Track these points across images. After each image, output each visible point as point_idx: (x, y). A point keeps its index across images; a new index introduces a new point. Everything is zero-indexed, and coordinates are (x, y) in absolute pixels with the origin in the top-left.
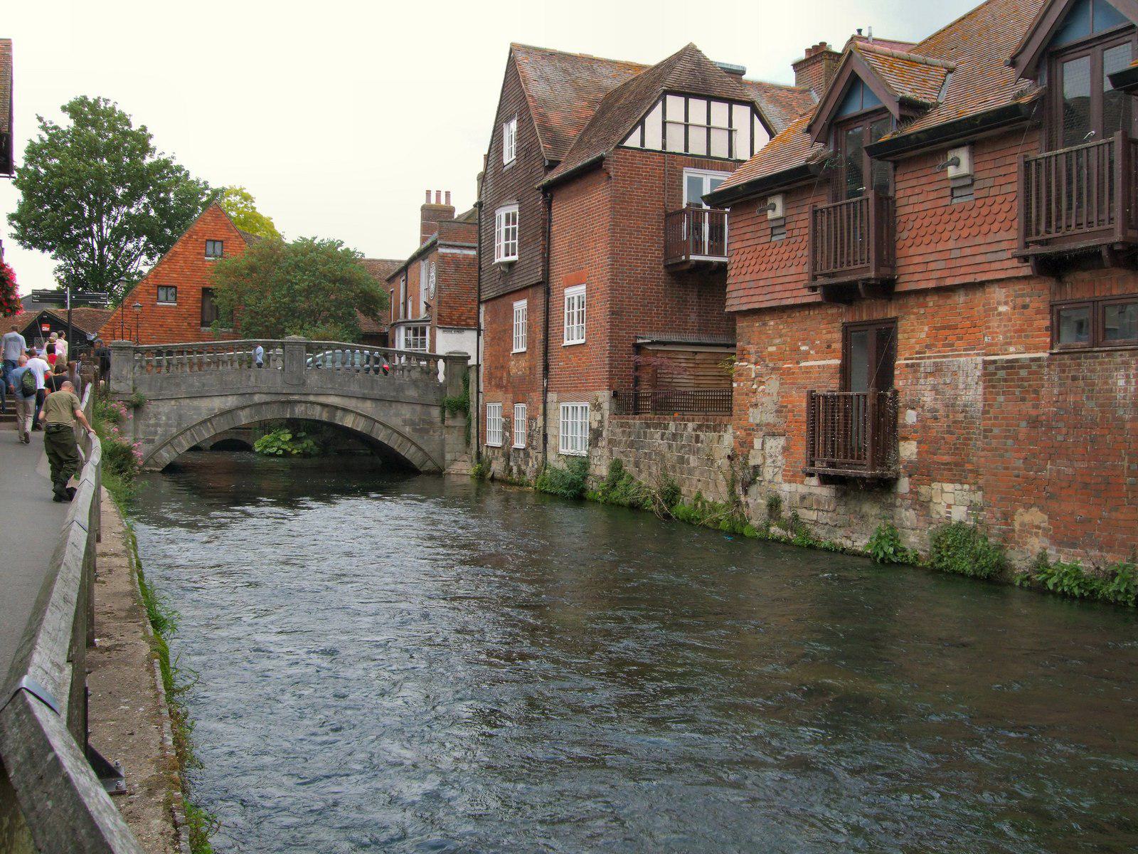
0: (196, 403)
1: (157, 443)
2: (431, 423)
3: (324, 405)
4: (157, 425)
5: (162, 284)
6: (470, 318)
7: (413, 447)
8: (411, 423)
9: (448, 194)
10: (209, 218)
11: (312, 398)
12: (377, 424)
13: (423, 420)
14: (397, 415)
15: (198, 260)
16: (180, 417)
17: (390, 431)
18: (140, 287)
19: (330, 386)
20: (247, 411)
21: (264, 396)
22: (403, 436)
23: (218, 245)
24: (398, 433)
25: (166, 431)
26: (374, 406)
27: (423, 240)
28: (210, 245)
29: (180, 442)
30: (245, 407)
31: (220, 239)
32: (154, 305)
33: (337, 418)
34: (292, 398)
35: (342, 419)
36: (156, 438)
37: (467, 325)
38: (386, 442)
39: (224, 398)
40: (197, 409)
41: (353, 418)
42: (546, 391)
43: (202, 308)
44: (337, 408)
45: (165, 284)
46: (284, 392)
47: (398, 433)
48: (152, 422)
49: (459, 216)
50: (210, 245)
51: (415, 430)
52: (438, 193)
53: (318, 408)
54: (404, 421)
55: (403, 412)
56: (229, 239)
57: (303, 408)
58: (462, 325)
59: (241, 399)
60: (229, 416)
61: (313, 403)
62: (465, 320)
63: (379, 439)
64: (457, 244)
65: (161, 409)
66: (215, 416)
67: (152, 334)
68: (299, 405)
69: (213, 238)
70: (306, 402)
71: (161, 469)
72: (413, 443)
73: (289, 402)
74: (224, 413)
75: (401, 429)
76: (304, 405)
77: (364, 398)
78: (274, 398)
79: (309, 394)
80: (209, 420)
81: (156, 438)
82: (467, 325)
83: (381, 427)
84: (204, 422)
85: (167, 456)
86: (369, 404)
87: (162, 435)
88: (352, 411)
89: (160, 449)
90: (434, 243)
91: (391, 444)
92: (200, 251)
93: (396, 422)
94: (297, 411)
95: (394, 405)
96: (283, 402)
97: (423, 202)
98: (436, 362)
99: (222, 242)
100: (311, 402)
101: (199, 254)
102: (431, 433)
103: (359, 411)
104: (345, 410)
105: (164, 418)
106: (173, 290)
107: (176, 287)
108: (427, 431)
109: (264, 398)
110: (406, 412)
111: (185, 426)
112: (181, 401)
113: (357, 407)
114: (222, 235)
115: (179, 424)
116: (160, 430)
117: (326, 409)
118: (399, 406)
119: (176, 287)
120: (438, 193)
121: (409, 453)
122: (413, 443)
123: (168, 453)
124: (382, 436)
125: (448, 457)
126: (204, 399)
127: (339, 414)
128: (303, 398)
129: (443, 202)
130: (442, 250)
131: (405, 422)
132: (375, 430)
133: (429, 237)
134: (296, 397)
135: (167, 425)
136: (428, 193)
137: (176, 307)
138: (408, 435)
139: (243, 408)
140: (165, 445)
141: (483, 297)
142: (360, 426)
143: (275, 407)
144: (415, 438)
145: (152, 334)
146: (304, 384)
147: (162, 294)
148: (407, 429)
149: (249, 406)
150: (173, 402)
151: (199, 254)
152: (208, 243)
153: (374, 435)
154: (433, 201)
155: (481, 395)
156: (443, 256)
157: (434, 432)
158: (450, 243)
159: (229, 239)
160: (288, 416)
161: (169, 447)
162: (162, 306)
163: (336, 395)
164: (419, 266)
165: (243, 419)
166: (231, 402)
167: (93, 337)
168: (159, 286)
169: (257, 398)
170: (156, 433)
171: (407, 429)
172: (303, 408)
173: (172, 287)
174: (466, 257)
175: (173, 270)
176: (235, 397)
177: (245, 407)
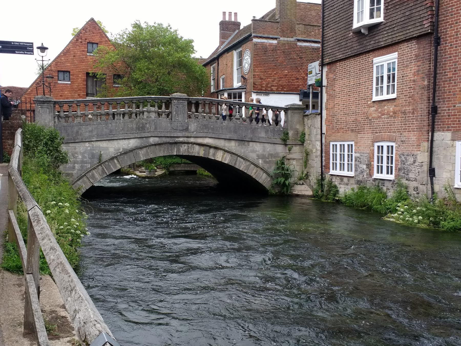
1: (75, 176)
5: (60, 69)
6: (273, 86)
8: (262, 157)
9: (236, 14)
11: (192, 140)
12: (239, 158)
14: (253, 151)
15: (83, 55)
17: (248, 163)
20: (145, 150)
23: (94, 45)
25: (82, 167)
26: (237, 145)
27: (222, 43)
29: (93, 175)
31: (96, 42)
33: (211, 154)
34: (177, 140)
35: (214, 155)
37: (272, 90)
38: (246, 172)
39: (126, 142)
41: (222, 154)
43: (87, 85)
44: (210, 147)
49: (245, 28)
50: (90, 45)
51: (265, 162)
52: (230, 13)
53: (197, 147)
54: (258, 156)
57: (186, 147)
58: (269, 91)
62: (270, 87)
63: (241, 169)
64: (266, 36)
66: (120, 155)
68: (183, 145)
70: (188, 143)
73: (176, 143)
74: (126, 152)
76: (186, 145)
77: (230, 140)
79: (191, 137)
81: (75, 172)
82: (272, 90)
83: (242, 160)
84: (112, 159)
87: (79, 170)
88: (221, 149)
90: (250, 35)
91: (249, 173)
92: (84, 49)
93: (253, 156)
94: (181, 150)
95: (251, 144)
96: (171, 143)
97: (221, 19)
98: (280, 112)
99: (97, 44)
101: (83, 51)
103: (226, 149)
104: (216, 148)
105: (80, 157)
106: (68, 73)
107: (69, 72)
109: (157, 140)
113: (225, 146)
116: (77, 166)
118: (254, 144)
119: (69, 72)
120: (230, 13)
123: (85, 183)
126: (112, 142)
127: (212, 151)
128: (185, 140)
129: (233, 19)
130: (255, 40)
131: (259, 157)
132: (238, 163)
133: (225, 41)
134: (181, 139)
135: (83, 162)
136: (224, 13)
137: (70, 84)
138: (261, 165)
139: (141, 148)
141: (327, 60)
142: (226, 159)
143: (166, 146)
146: (187, 129)
147: (61, 75)
148: (260, 161)
150: (87, 144)
151: (83, 51)
153: (237, 167)
154: (227, 19)
155: (323, 136)
156: (256, 44)
158: (260, 35)
160: (175, 154)
161: (85, 178)
162: (61, 84)
164: (232, 55)
165: (142, 157)
166: (132, 143)
168: (58, 71)
169: (152, 140)
170: (74, 168)
172: (186, 147)
174: (271, 45)
176: (135, 140)
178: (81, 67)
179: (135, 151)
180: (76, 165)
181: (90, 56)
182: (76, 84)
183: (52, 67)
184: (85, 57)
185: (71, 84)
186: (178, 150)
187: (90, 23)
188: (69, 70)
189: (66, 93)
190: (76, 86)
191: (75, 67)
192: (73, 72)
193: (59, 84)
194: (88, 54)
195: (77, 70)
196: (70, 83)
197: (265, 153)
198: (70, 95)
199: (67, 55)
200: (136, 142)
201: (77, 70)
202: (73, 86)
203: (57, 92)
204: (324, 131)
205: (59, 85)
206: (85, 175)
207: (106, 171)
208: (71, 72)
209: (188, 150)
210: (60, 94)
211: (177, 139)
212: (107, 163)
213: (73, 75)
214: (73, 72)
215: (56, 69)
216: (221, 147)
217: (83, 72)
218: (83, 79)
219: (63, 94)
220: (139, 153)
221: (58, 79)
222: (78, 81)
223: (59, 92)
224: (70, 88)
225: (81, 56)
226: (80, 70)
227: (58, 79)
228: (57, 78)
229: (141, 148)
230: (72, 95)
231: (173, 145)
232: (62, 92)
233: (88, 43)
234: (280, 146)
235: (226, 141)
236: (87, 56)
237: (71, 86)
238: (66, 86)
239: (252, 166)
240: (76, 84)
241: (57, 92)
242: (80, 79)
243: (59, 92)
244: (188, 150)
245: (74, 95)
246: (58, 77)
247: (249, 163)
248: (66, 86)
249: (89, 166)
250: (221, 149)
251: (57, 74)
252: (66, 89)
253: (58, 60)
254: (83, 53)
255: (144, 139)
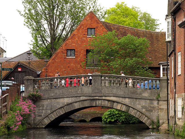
0: (58, 100)
2: (153, 107)
3: (109, 101)
4: (43, 110)
7: (146, 118)
10: (89, 18)
11: (104, 98)
12: (130, 108)
13: (150, 107)
14: (139, 104)
16: (52, 106)
18: (59, 50)
19: (111, 93)
21: (84, 97)
22: (141, 113)
24: (139, 112)
25: (46, 112)
28: (89, 30)
29: (51, 116)
30: (77, 102)
31: (94, 27)
32: (65, 58)
34: (95, 98)
36: (42, 115)
38: (134, 115)
39: (68, 98)
40: (58, 103)
42: (175, 93)
44: (114, 102)
45: (70, 48)
46: (92, 95)
47: (139, 112)
48: (41, 108)
50: (89, 30)
51: (146, 110)
53: (107, 102)
55: (142, 103)
56: (97, 27)
59: (75, 98)
60: (71, 105)
61: (104, 100)
65: (44, 103)
67: (65, 71)
69: (91, 27)
70: (101, 100)
71: (44, 127)
72: (146, 116)
73: (94, 100)
74: (68, 104)
75: (141, 110)
78: (89, 98)
80: (63, 107)
83: (133, 109)
84: (61, 108)
85: (47, 121)
86: (127, 99)
88: (120, 103)
89: (44, 119)
92: (85, 33)
93: (139, 107)
94: (97, 103)
95: (138, 100)
96: (92, 100)
99: (95, 28)
100: (103, 100)
102: (154, 111)
106: (74, 51)
108: (152, 111)
109: (84, 98)
110: (143, 103)
111: (54, 110)
112: (52, 100)
113: (122, 101)
114: (94, 26)
115: (51, 109)
117: (110, 102)
118: (140, 100)
119: (75, 50)
121: (144, 120)
122: (146, 116)
124: (132, 112)
125: (161, 121)
127: (115, 104)
131: (143, 107)
132: (130, 111)
134: (97, 98)
135: (46, 109)
139: (76, 102)
140: (46, 117)
142: (124, 108)
144: (147, 114)
145: (65, 71)
146: (101, 91)
148: (144, 110)
149: (78, 101)
150: (49, 100)
152: (89, 30)
157: (155, 111)
159: (97, 27)
161: (47, 118)
163: (114, 96)
167: (40, 73)
168: (67, 50)
169: (82, 98)
170: (42, 112)
171: (144, 110)
173: (73, 50)
175: (72, 42)
176: (73, 98)
177: (77, 102)
178: (83, 46)
179: (73, 104)
180: (43, 111)
181: (89, 37)
182: (79, 58)
183: (63, 47)
184: (85, 38)
185: (76, 58)
186: (96, 103)
187: (89, 14)
188: (74, 48)
189: (72, 65)
190: (79, 60)
191: (79, 46)
192: (77, 50)
193: (67, 59)
194: (88, 36)
195: (80, 48)
196: (75, 57)
197: (146, 105)
198: (75, 66)
199: (73, 38)
200: (73, 99)
201: (80, 48)
202: (77, 60)
203: (66, 64)
204: (169, 93)
205: (67, 59)
206: (47, 116)
207: (58, 114)
208: (76, 50)
209: (101, 103)
210: (68, 66)
211: (95, 98)
212: (58, 110)
213: (77, 52)
214: (77, 50)
215: (66, 48)
216: (120, 102)
217: (84, 50)
218: (84, 55)
219: (70, 66)
220: (75, 105)
221: (67, 55)
222: (81, 56)
223: (67, 64)
224: (74, 61)
225: (83, 38)
226: (82, 48)
227: (67, 55)
228: (66, 54)
229: (76, 102)
230: (76, 66)
231: (93, 101)
232: (69, 65)
233: (88, 28)
234: (156, 101)
235: (123, 99)
236: (87, 38)
237: (75, 60)
238: (72, 60)
239: (138, 112)
240: (79, 58)
241: (66, 64)
242: (82, 55)
243: (67, 64)
244: (101, 103)
245: (77, 66)
246: (67, 54)
247: (136, 111)
248: (72, 60)
249: (50, 112)
250: (120, 103)
251: (66, 52)
252: (72, 62)
253: (68, 42)
254: (85, 36)
255: (78, 97)
